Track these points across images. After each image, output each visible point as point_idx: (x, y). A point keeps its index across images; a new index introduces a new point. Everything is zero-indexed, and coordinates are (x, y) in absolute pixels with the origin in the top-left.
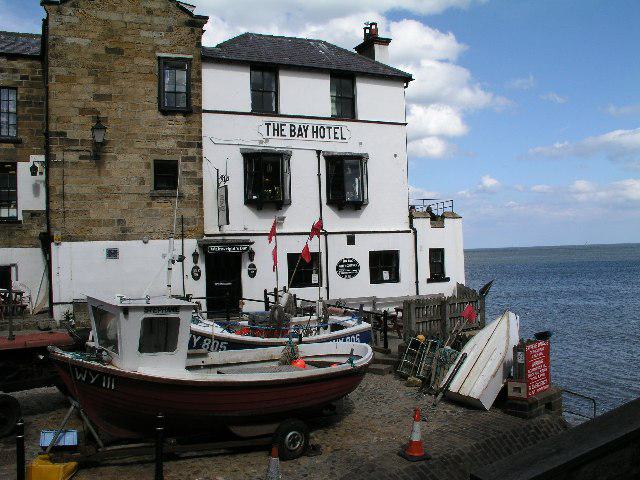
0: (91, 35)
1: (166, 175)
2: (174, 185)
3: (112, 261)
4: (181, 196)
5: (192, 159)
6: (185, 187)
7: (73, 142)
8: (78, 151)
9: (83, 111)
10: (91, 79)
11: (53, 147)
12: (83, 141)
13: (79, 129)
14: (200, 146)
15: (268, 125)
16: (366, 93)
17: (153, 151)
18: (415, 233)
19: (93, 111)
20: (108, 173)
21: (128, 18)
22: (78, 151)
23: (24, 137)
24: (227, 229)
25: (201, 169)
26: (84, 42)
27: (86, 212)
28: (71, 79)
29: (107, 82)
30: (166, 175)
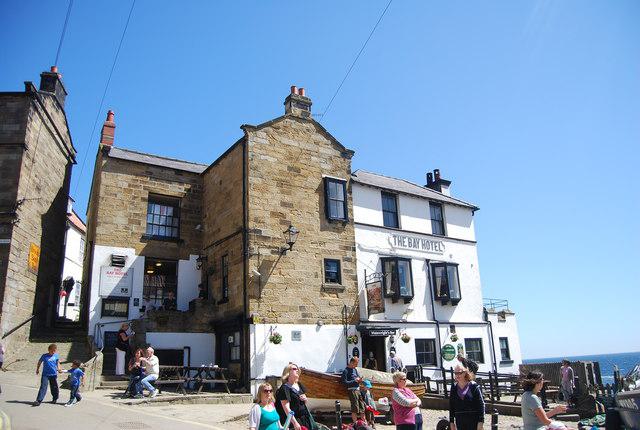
0: (278, 156)
1: (333, 273)
5: (349, 260)
6: (346, 282)
7: (266, 238)
8: (270, 247)
9: (274, 214)
10: (275, 189)
11: (252, 245)
15: (395, 236)
19: (282, 215)
21: (302, 145)
22: (270, 247)
26: (271, 160)
28: (264, 190)
29: (289, 193)
30: (333, 273)
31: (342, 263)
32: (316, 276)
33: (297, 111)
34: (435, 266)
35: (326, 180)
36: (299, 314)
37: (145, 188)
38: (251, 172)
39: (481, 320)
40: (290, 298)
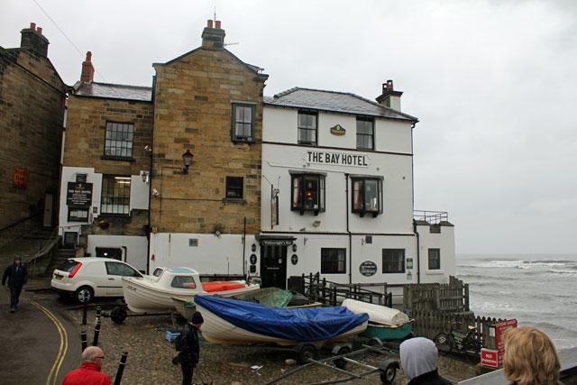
0: (186, 87)
1: (235, 187)
2: (241, 196)
3: (193, 248)
4: (244, 203)
5: (254, 177)
7: (169, 161)
9: (177, 141)
10: (184, 118)
11: (155, 165)
12: (177, 161)
13: (174, 152)
14: (260, 167)
15: (310, 153)
16: (381, 128)
17: (226, 170)
18: (418, 236)
20: (193, 185)
23: (137, 158)
24: (276, 228)
25: (260, 183)
26: (178, 92)
27: (177, 212)
28: (170, 118)
30: (235, 187)
31: (245, 180)
32: (217, 192)
33: (210, 44)
34: (355, 179)
35: (233, 104)
36: (198, 224)
37: (103, 118)
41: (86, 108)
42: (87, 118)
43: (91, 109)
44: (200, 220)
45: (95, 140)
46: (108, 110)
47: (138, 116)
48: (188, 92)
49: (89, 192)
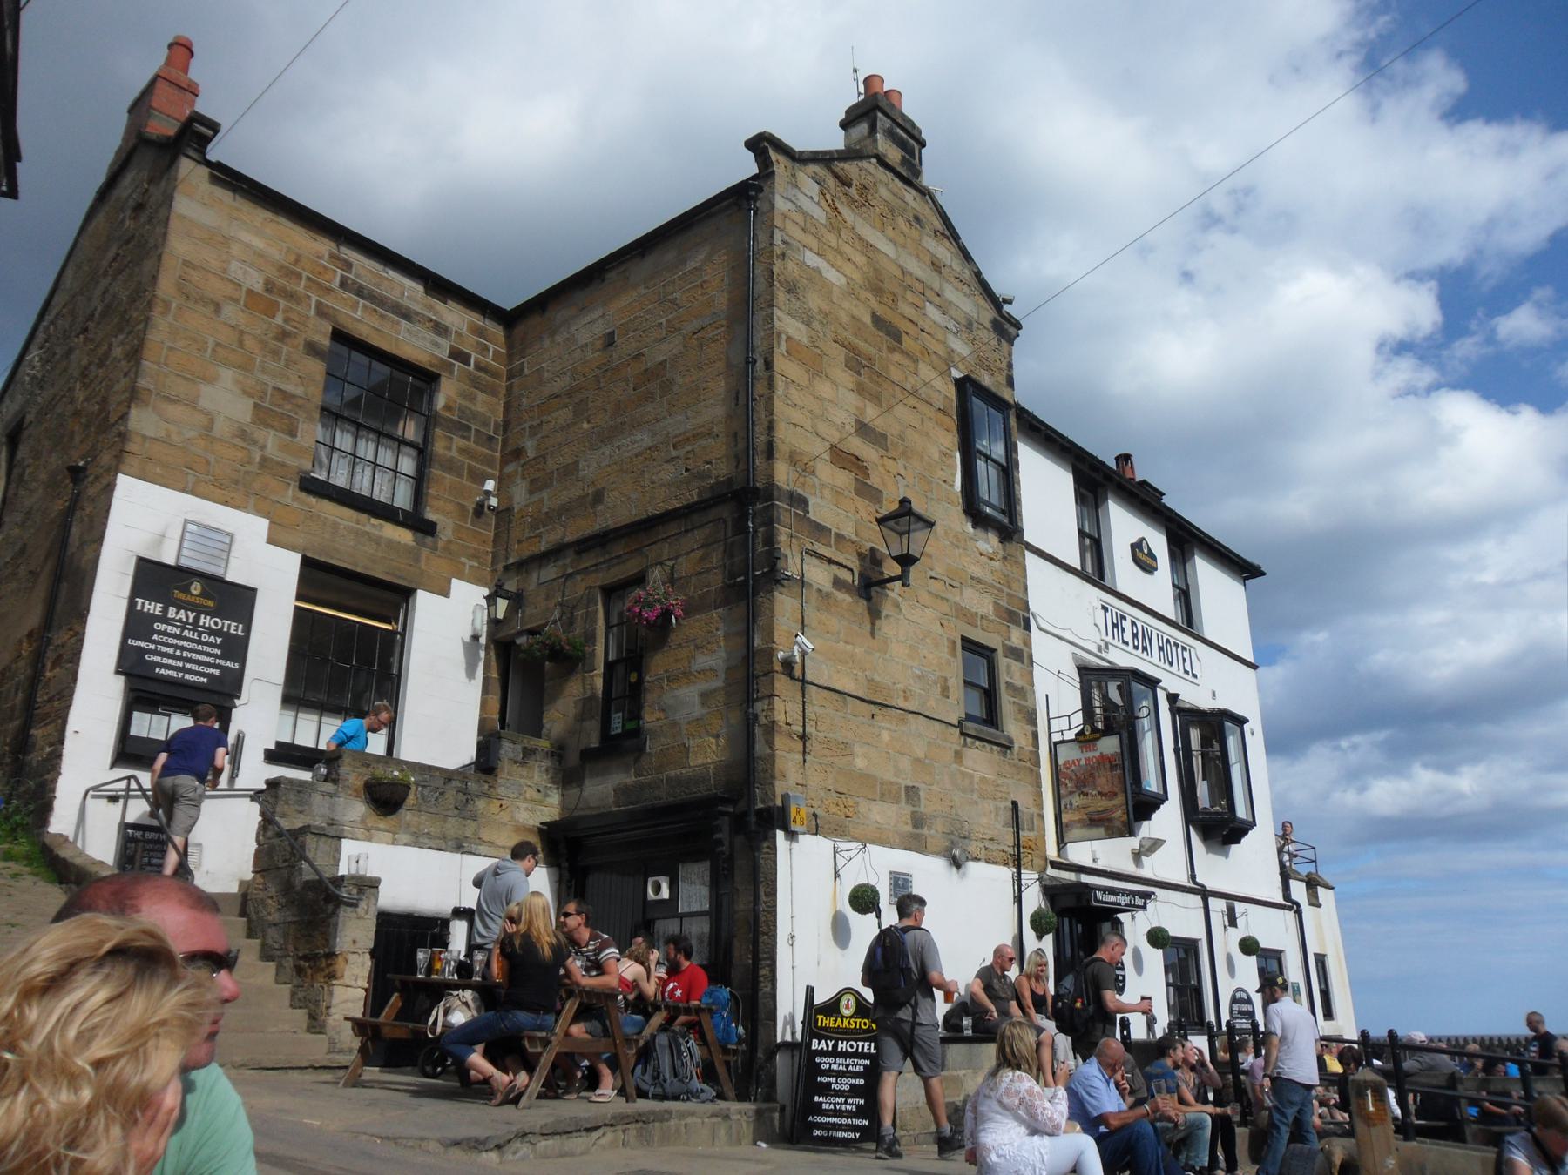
0: (849, 269)
4: (1007, 747)
6: (1012, 727)
7: (819, 530)
8: (830, 561)
9: (842, 458)
10: (845, 378)
12: (840, 537)
14: (1027, 627)
15: (1105, 609)
18: (1299, 913)
26: (832, 275)
27: (846, 750)
29: (876, 399)
30: (988, 694)
32: (945, 692)
36: (906, 810)
37: (322, 312)
38: (781, 296)
39: (1279, 899)
40: (882, 750)
41: (258, 243)
42: (259, 287)
43: (276, 254)
44: (911, 793)
45: (286, 396)
46: (344, 284)
47: (459, 355)
48: (851, 293)
49: (235, 628)
